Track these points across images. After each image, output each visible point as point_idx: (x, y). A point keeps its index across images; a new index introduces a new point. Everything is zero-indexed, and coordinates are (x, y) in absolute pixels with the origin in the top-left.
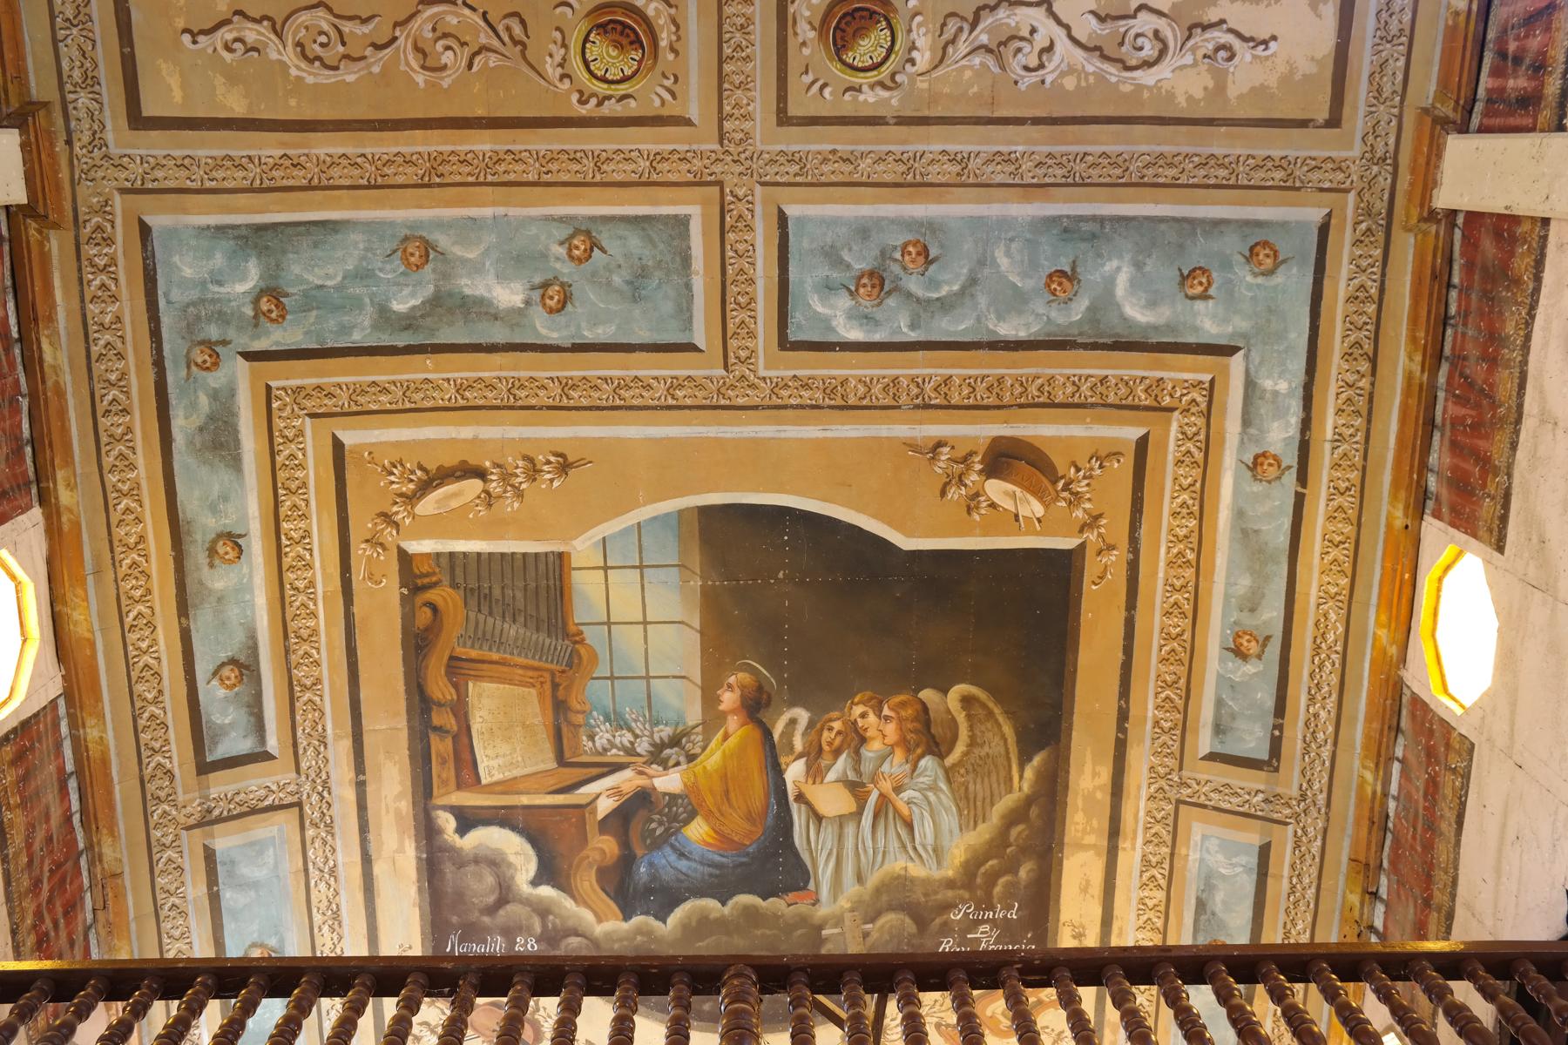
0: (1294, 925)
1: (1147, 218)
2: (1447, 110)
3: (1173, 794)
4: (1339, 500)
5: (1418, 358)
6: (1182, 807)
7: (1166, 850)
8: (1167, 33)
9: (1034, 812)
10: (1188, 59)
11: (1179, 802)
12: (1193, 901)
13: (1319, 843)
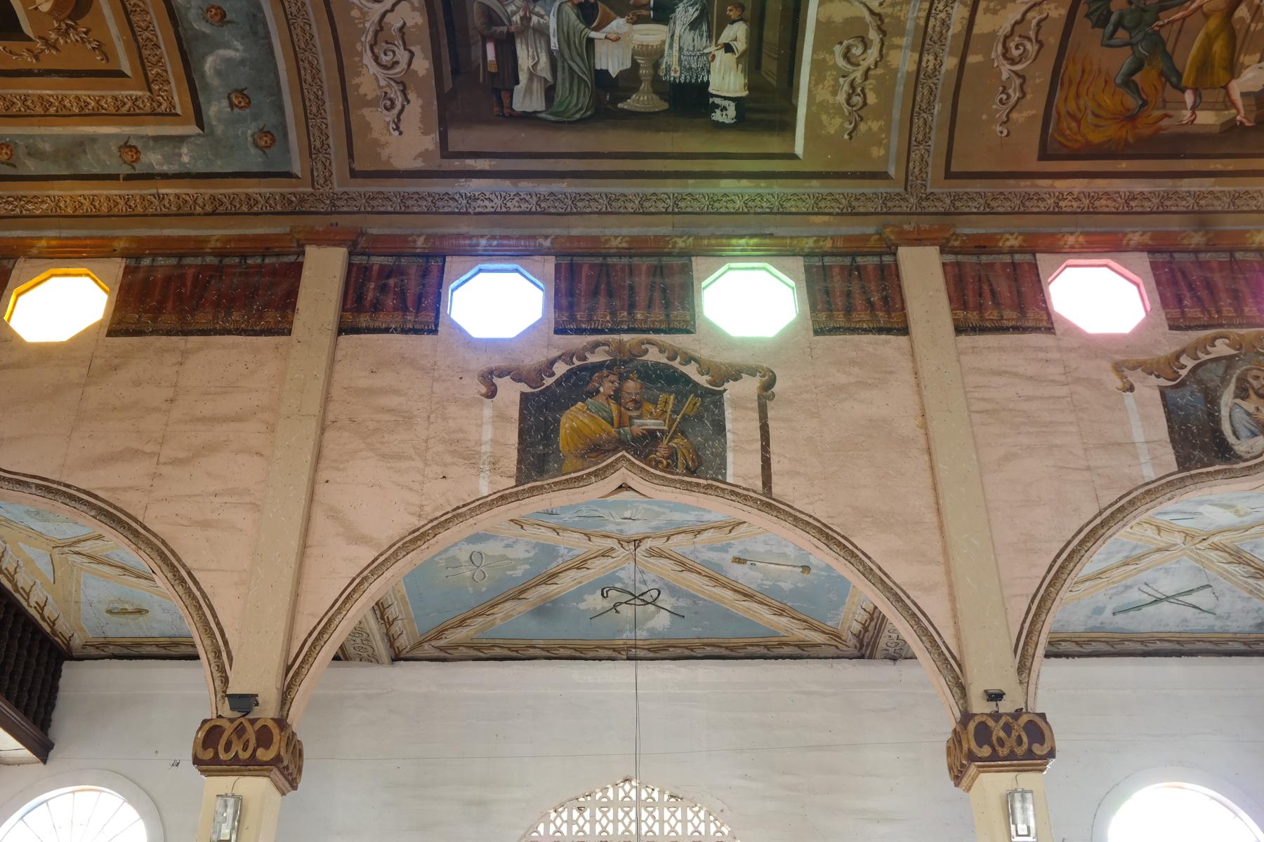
1: (276, 65)
2: (362, 242)
4: (122, 202)
5: (219, 245)
8: (398, 69)
10: (383, 83)
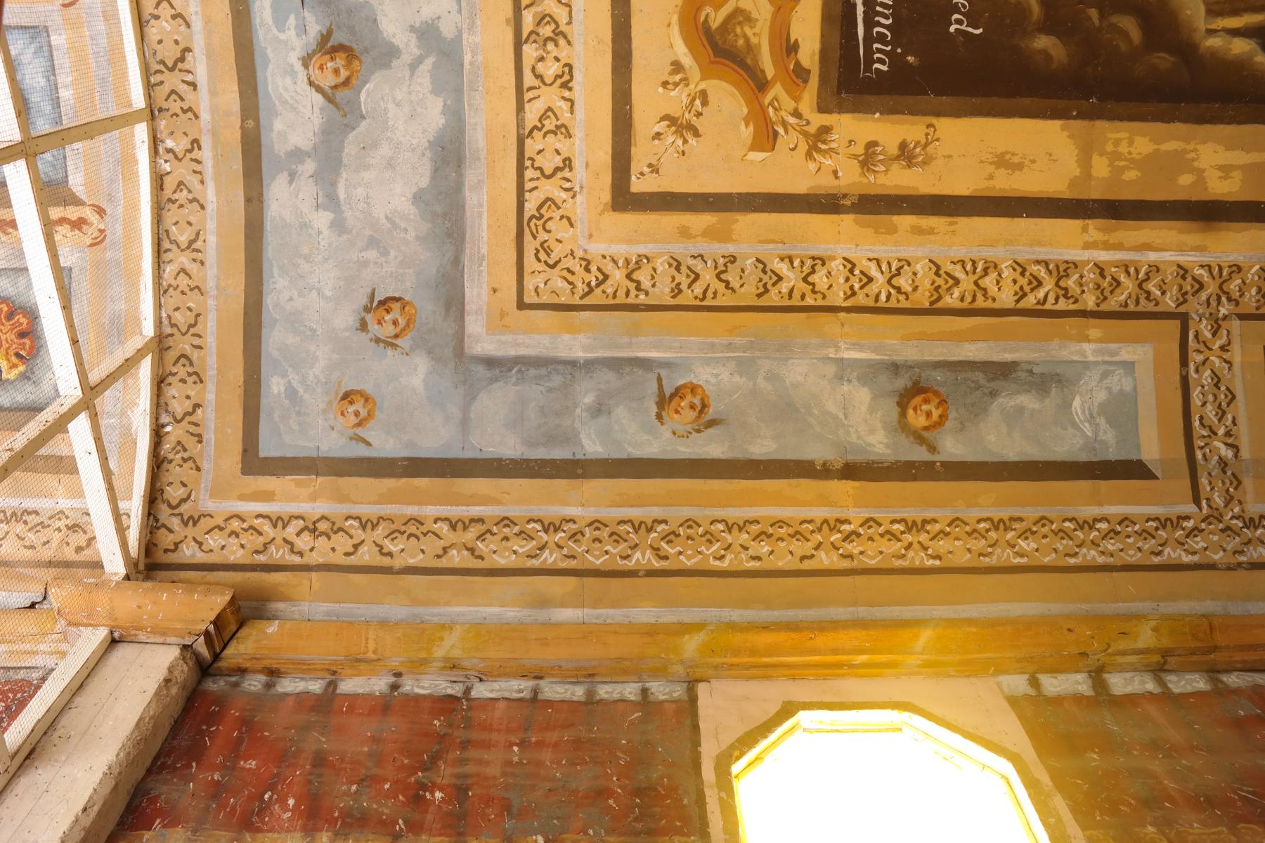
0: (1023, 535)
3: (1195, 306)
6: (1177, 323)
7: (1090, 301)
9: (1163, 60)
11: (1184, 319)
12: (1008, 357)
13: (1187, 559)
